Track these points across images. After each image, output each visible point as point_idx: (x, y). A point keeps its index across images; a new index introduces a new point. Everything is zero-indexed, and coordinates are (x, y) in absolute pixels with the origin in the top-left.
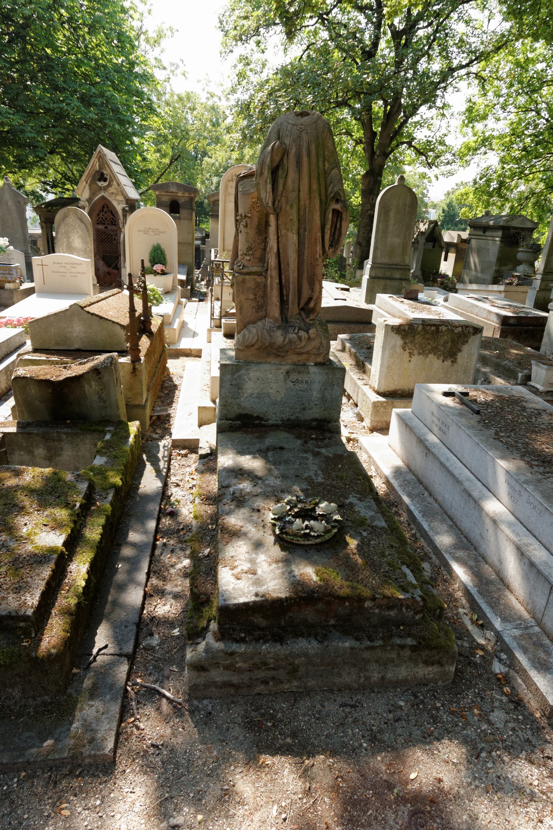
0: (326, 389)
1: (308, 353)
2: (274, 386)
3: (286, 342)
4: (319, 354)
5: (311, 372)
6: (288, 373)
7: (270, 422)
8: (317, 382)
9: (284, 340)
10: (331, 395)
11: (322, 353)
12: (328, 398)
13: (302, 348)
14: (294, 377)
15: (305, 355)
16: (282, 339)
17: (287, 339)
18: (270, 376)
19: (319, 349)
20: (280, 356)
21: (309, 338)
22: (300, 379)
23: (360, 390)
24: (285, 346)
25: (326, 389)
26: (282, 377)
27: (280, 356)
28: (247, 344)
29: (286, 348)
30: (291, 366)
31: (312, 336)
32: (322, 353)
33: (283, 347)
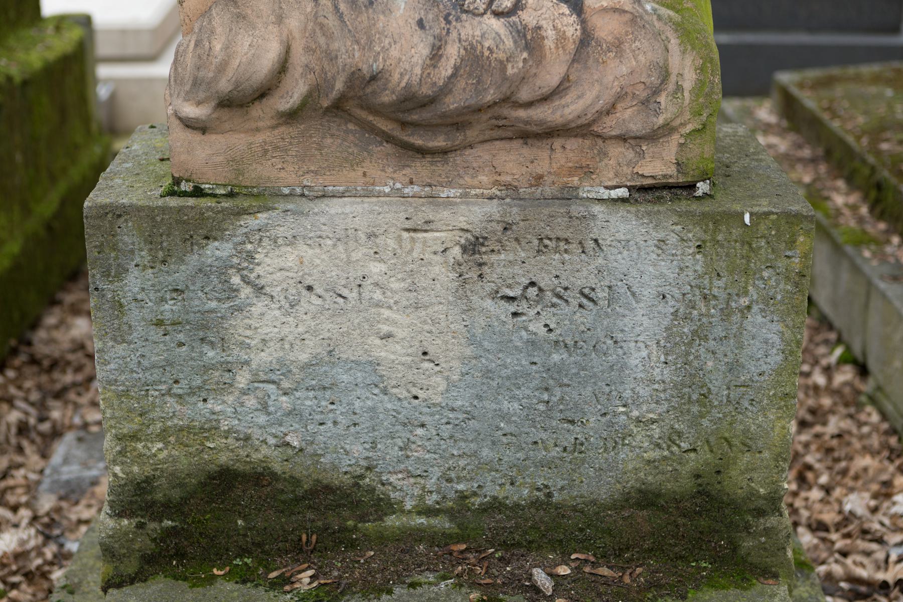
0: (699, 335)
1: (582, 130)
2: (400, 323)
3: (445, 70)
4: (654, 136)
5: (606, 239)
6: (474, 246)
7: (392, 521)
8: (648, 293)
9: (436, 55)
10: (734, 367)
11: (668, 129)
12: (717, 384)
13: (545, 99)
14: (509, 265)
15: (573, 144)
16: (423, 50)
17: (453, 52)
18: (376, 268)
19: (648, 103)
20: (422, 152)
21: (586, 39)
22: (545, 281)
23: (876, 303)
24: (446, 89)
25: (699, 335)
26: (441, 274)
27: (422, 152)
28: (224, 85)
29: (452, 103)
30: (493, 208)
31: (606, 28)
32: (668, 129)
33: (431, 101)
